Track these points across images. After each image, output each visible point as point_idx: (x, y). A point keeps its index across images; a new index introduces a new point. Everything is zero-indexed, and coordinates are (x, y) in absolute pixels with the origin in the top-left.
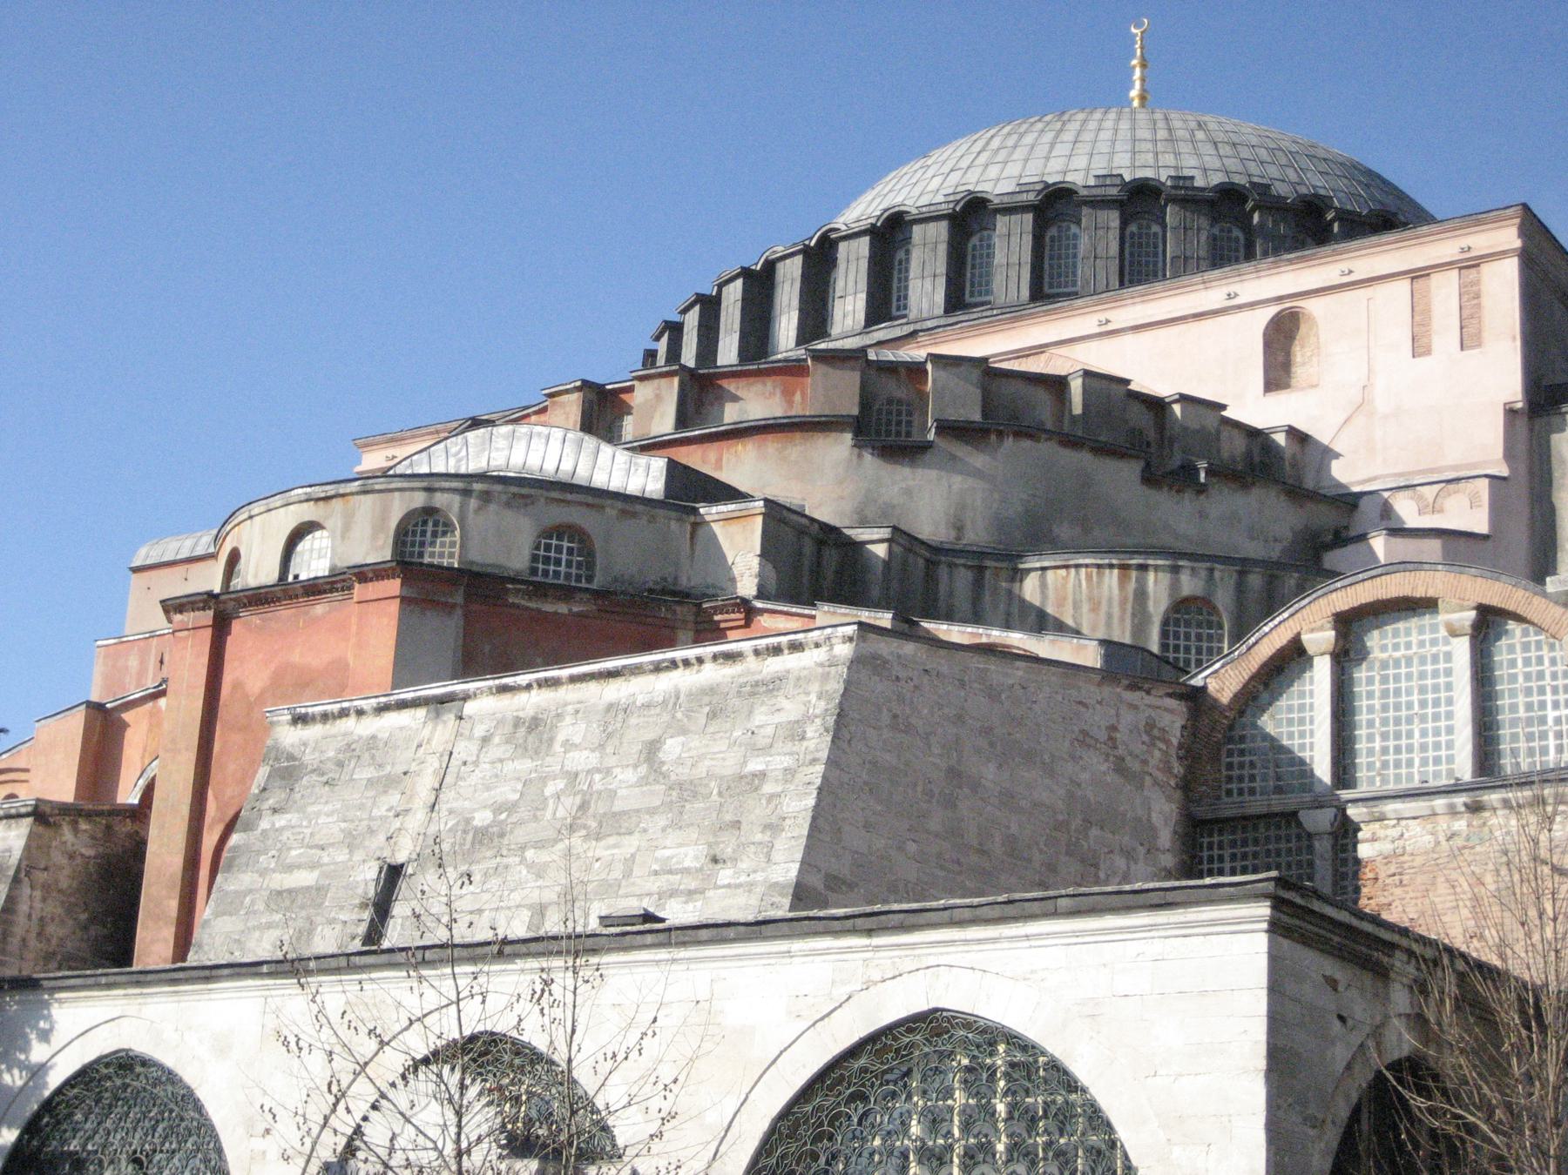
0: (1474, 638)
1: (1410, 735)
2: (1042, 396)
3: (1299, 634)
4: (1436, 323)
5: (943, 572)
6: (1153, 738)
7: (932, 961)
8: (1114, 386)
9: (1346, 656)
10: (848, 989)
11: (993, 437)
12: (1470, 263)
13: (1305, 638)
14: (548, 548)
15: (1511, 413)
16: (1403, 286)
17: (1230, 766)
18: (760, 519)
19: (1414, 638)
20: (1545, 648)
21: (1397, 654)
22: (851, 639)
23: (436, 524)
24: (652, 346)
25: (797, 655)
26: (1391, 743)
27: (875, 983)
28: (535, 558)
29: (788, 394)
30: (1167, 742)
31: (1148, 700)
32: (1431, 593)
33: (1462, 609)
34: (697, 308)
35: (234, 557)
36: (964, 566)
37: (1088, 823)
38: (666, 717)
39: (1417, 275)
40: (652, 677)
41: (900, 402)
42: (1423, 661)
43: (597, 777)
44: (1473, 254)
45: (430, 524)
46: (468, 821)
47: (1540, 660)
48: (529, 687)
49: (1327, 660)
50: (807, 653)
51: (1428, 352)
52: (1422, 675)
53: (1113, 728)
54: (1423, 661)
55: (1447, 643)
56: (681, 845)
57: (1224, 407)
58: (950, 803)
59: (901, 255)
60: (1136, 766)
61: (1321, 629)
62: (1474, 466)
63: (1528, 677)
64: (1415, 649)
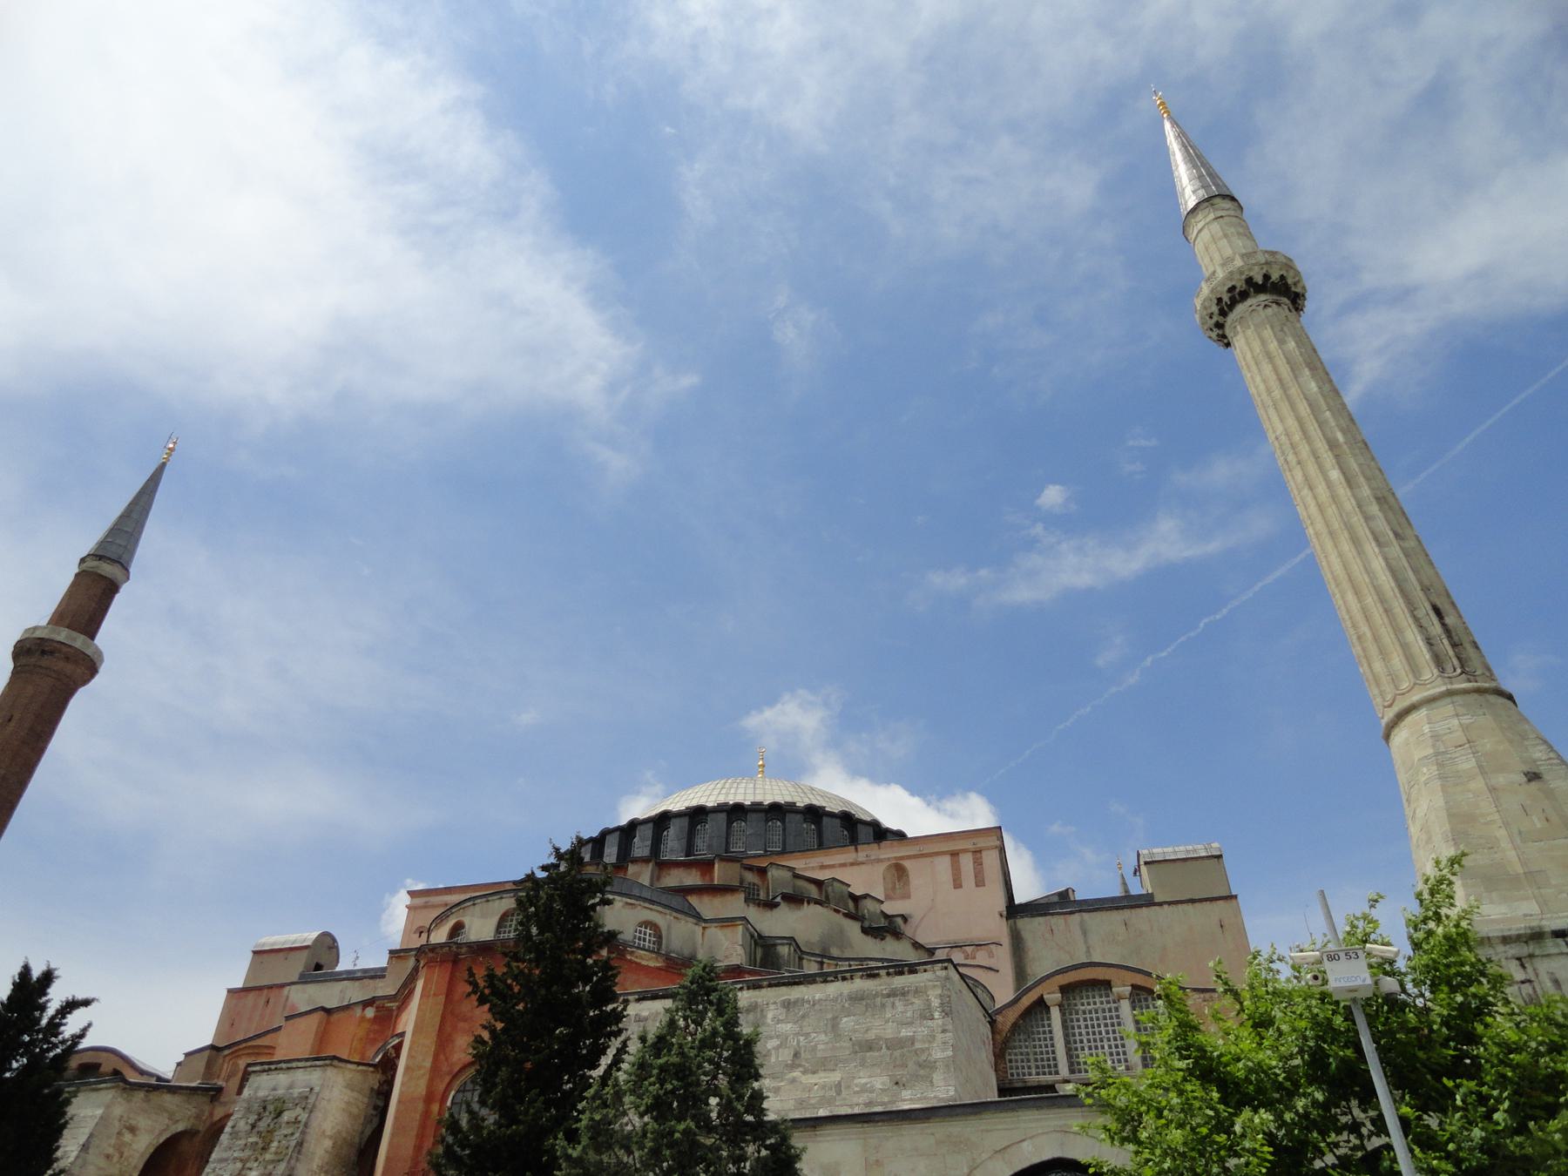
3: (1042, 995)
5: (805, 961)
11: (806, 904)
13: (1045, 997)
14: (640, 932)
17: (1010, 1061)
21: (1089, 1007)
22: (946, 968)
29: (703, 875)
32: (1107, 978)
33: (1124, 986)
36: (815, 961)
38: (839, 1006)
39: (954, 854)
41: (754, 884)
42: (1104, 1011)
43: (802, 1038)
51: (961, 886)
52: (1105, 1018)
54: (1104, 1011)
55: (1114, 1002)
56: (870, 1077)
59: (665, 833)
61: (1053, 993)
64: (1098, 1005)
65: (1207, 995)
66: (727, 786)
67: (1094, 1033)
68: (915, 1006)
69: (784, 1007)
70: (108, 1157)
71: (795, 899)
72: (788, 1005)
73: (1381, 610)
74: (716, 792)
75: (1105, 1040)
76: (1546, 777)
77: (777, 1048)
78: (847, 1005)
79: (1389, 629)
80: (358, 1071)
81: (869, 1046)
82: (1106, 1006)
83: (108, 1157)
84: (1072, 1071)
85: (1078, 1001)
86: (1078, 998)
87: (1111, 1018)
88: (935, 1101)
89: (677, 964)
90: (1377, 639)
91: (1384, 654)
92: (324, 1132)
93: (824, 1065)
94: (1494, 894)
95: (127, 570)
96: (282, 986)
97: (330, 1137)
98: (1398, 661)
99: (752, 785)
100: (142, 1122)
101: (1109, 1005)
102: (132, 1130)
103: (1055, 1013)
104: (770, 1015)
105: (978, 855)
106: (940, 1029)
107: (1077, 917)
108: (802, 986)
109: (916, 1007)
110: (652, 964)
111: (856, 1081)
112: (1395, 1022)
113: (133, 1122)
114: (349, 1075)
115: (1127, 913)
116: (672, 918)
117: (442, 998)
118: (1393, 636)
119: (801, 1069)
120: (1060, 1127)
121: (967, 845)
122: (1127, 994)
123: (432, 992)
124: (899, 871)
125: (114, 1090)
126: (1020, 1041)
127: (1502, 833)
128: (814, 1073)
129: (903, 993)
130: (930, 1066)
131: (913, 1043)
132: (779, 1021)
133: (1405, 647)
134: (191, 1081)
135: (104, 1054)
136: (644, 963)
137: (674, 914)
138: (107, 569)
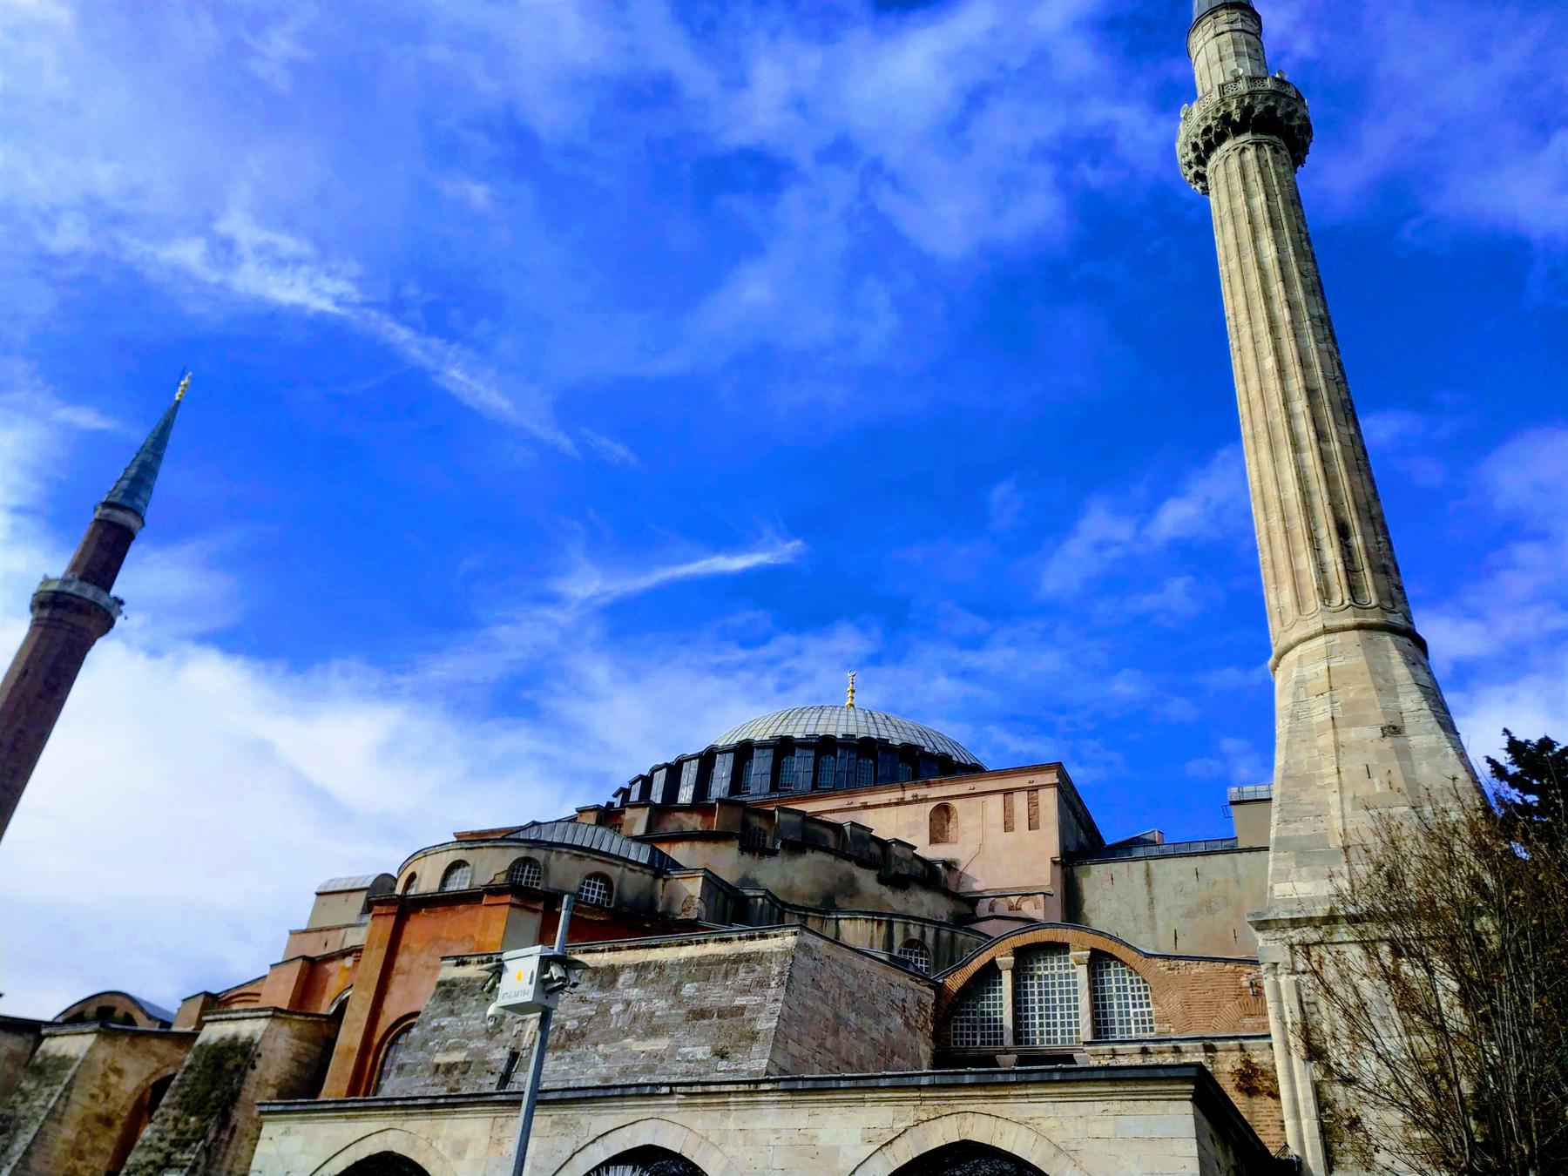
0: (1088, 966)
1: (1055, 1016)
2: (829, 833)
4: (1016, 817)
6: (920, 1008)
7: (962, 1108)
8: (865, 832)
9: (1021, 973)
10: (905, 1125)
12: (1034, 789)
15: (1054, 863)
16: (1000, 797)
18: (701, 879)
19: (1055, 964)
20: (1127, 974)
21: (1046, 973)
22: (795, 934)
23: (530, 867)
24: (614, 800)
25: (763, 941)
26: (1045, 1021)
27: (923, 1122)
28: (582, 890)
30: (926, 1011)
31: (919, 987)
32: (1065, 941)
33: (1083, 950)
35: (412, 877)
37: (893, 1053)
39: (1008, 792)
41: (760, 829)
43: (643, 1004)
44: (1034, 784)
47: (1124, 981)
48: (603, 951)
49: (1010, 972)
50: (769, 940)
51: (1013, 830)
52: (1061, 984)
53: (904, 1000)
54: (1060, 976)
55: (1073, 967)
56: (694, 1046)
57: (915, 848)
58: (836, 1032)
60: (914, 1024)
61: (1006, 955)
62: (1037, 887)
63: (1118, 989)
65: (1173, 963)
68: (756, 974)
69: (636, 971)
70: (93, 1097)
71: (795, 848)
72: (641, 968)
75: (1058, 1009)
76: (1408, 731)
77: (618, 1014)
80: (309, 1022)
81: (701, 1014)
82: (1064, 972)
83: (93, 1097)
84: (1017, 1040)
87: (1068, 984)
88: (745, 1074)
92: (266, 1081)
93: (654, 1032)
94: (1304, 871)
95: (143, 519)
96: (339, 928)
97: (273, 1086)
100: (127, 1064)
101: (1067, 971)
102: (119, 1072)
103: (1007, 977)
104: (621, 979)
105: (1035, 794)
106: (772, 999)
107: (1142, 864)
108: (658, 950)
111: (680, 1050)
112: (434, 1045)
113: (119, 1065)
114: (296, 1026)
115: (1198, 861)
117: (383, 952)
120: (658, 1114)
121: (1022, 781)
122: (1086, 960)
123: (375, 945)
124: (942, 813)
125: (95, 1035)
126: (968, 1006)
127: (1334, 799)
128: (643, 1040)
130: (754, 1037)
131: (742, 1014)
132: (629, 986)
134: (186, 1027)
135: (118, 998)
137: (630, 866)
138: (120, 516)
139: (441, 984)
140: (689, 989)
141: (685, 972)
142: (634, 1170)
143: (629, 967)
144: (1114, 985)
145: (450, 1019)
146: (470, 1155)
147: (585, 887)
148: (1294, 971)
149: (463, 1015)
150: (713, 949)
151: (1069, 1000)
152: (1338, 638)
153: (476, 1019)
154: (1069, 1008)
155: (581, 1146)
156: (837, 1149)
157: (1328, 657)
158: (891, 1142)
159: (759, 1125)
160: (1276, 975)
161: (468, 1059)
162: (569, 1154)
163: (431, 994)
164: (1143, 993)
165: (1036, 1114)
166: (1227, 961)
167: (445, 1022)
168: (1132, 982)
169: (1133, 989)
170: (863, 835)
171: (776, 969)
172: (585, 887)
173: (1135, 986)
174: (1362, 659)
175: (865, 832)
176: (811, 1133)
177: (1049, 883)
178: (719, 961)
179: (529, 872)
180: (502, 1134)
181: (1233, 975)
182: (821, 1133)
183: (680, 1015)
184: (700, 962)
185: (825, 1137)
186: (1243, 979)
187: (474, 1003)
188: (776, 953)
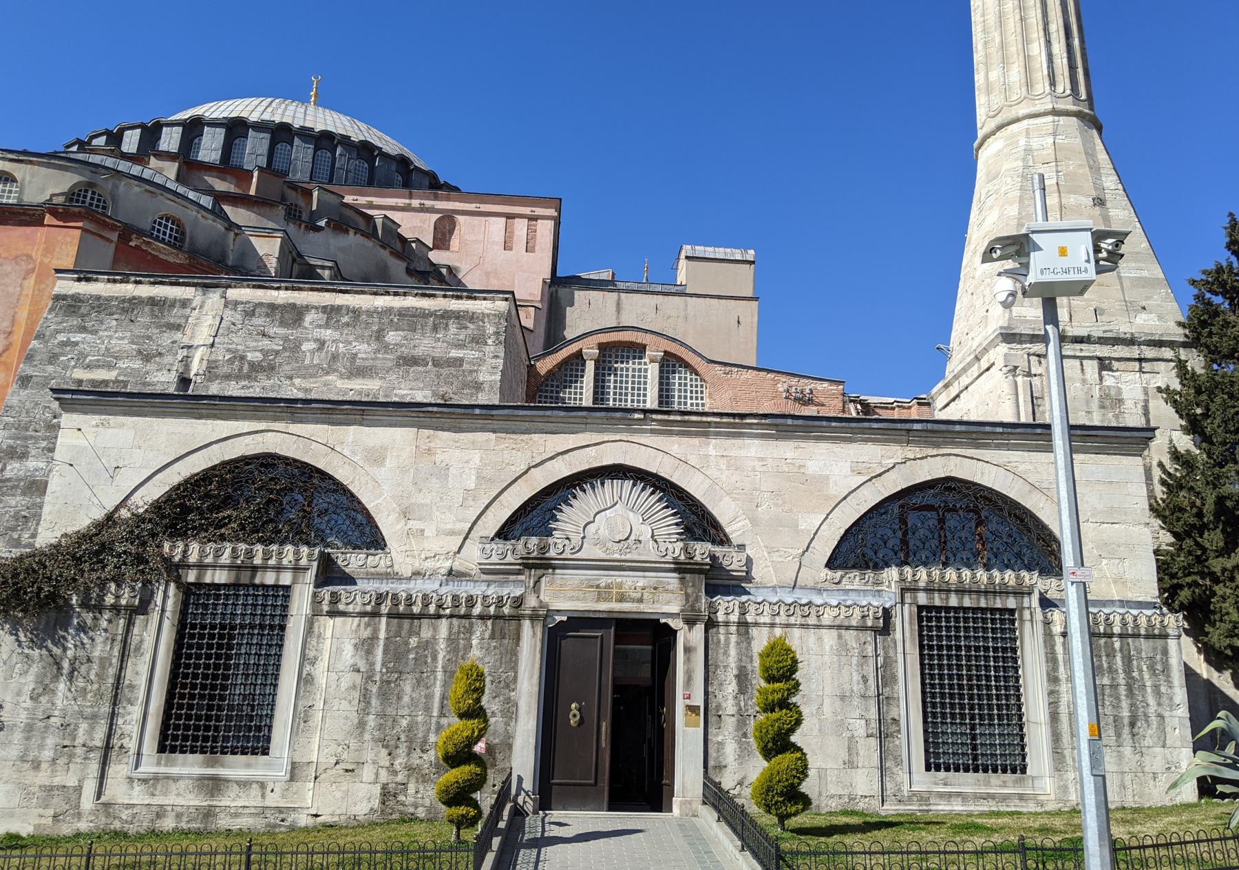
0: (661, 367)
15: (544, 282)
16: (503, 220)
18: (279, 240)
22: (506, 299)
23: (94, 193)
34: (139, 131)
39: (510, 217)
40: (372, 297)
41: (296, 206)
43: (341, 345)
45: (90, 193)
46: (242, 358)
48: (278, 288)
50: (478, 302)
51: (511, 249)
56: (411, 389)
61: (592, 348)
65: (728, 369)
66: (274, 105)
67: (621, 388)
68: (469, 332)
69: (324, 312)
72: (331, 312)
73: (1018, 17)
74: (261, 109)
77: (313, 352)
78: (396, 320)
79: (1019, 38)
81: (413, 361)
85: (613, 359)
86: (614, 356)
89: (202, 265)
90: (1003, 46)
91: (1005, 62)
98: (1016, 73)
99: (303, 110)
103: (590, 367)
106: (491, 355)
107: (615, 295)
109: (469, 332)
110: (171, 259)
116: (199, 216)
118: (1020, 46)
119: (336, 374)
121: (526, 210)
128: (349, 378)
129: (458, 316)
131: (461, 365)
132: (320, 326)
133: (1027, 59)
136: (161, 256)
139: (57, 298)
140: (392, 337)
141: (385, 320)
142: (634, 485)
143: (316, 308)
144: (677, 381)
145: (83, 335)
146: (389, 463)
147: (157, 227)
148: (1029, 374)
149: (101, 333)
150: (411, 302)
151: (639, 389)
152: (1063, 120)
153: (122, 338)
154: (639, 395)
155: (538, 461)
156: (827, 478)
157: (1055, 134)
158: (880, 475)
159: (743, 453)
160: (1014, 376)
161: (121, 378)
162: (524, 467)
163: (982, 249)
164: (699, 389)
165: (1013, 459)
166: (769, 371)
167: (77, 337)
168: (691, 380)
169: (691, 386)
170: (391, 227)
171: (490, 329)
172: (157, 227)
173: (694, 383)
174: (1079, 140)
175: (394, 227)
176: (798, 463)
177: (539, 299)
178: (424, 314)
179: (92, 199)
180: (432, 445)
181: (772, 382)
182: (809, 463)
183: (389, 359)
184: (403, 313)
185: (813, 467)
186: (779, 385)
187: (114, 323)
188: (488, 315)
